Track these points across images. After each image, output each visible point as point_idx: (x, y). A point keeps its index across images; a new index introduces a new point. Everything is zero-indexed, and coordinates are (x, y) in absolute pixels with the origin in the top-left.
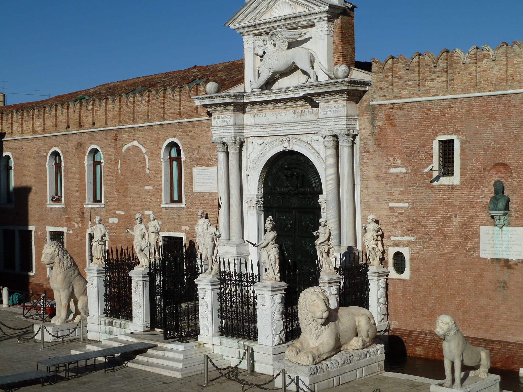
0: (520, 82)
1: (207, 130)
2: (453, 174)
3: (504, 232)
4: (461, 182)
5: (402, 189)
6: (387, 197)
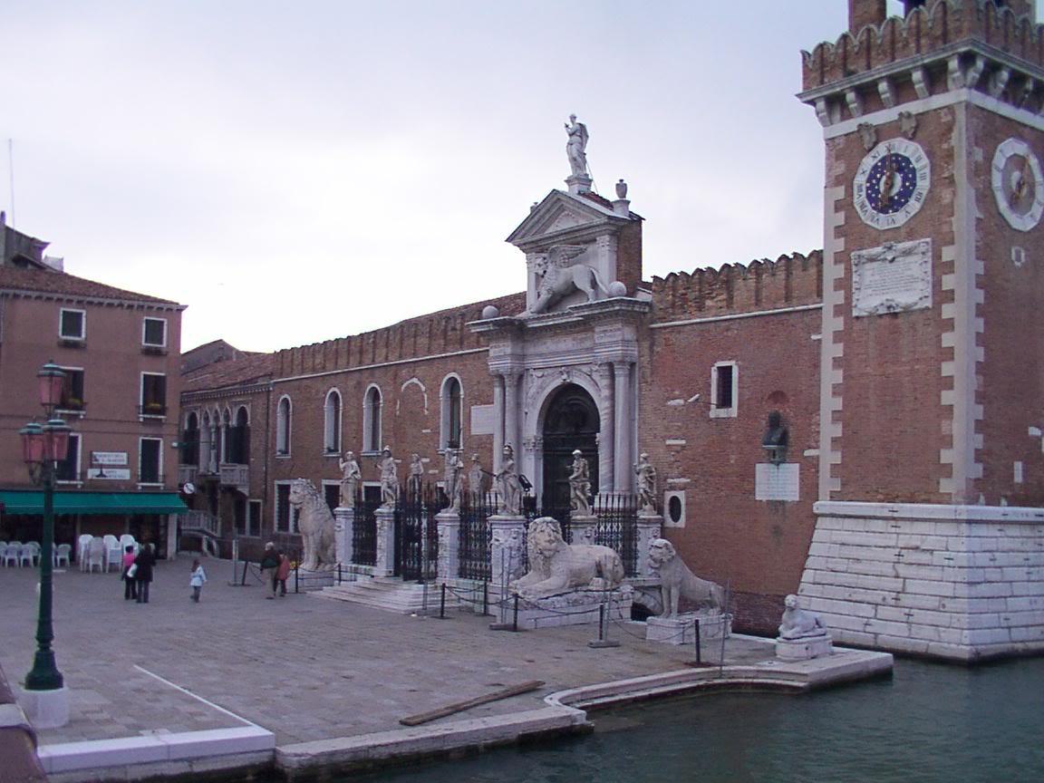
2: (731, 406)
3: (780, 470)
4: (739, 416)
5: (679, 424)
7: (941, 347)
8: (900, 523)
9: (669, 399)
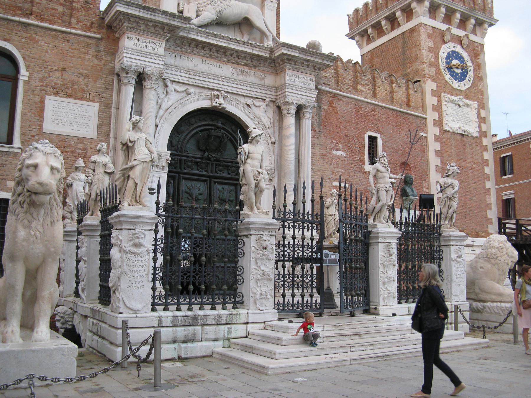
0: (414, 108)
1: (84, 50)
6: (331, 176)
7: (483, 158)
8: (475, 249)
9: (333, 149)
